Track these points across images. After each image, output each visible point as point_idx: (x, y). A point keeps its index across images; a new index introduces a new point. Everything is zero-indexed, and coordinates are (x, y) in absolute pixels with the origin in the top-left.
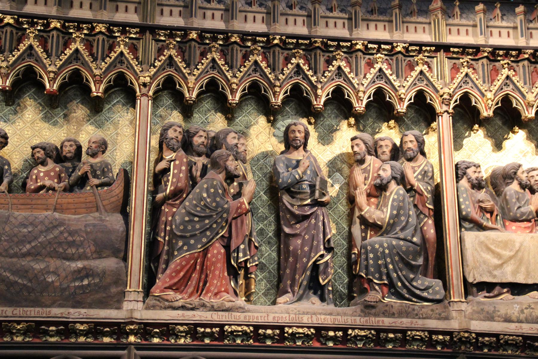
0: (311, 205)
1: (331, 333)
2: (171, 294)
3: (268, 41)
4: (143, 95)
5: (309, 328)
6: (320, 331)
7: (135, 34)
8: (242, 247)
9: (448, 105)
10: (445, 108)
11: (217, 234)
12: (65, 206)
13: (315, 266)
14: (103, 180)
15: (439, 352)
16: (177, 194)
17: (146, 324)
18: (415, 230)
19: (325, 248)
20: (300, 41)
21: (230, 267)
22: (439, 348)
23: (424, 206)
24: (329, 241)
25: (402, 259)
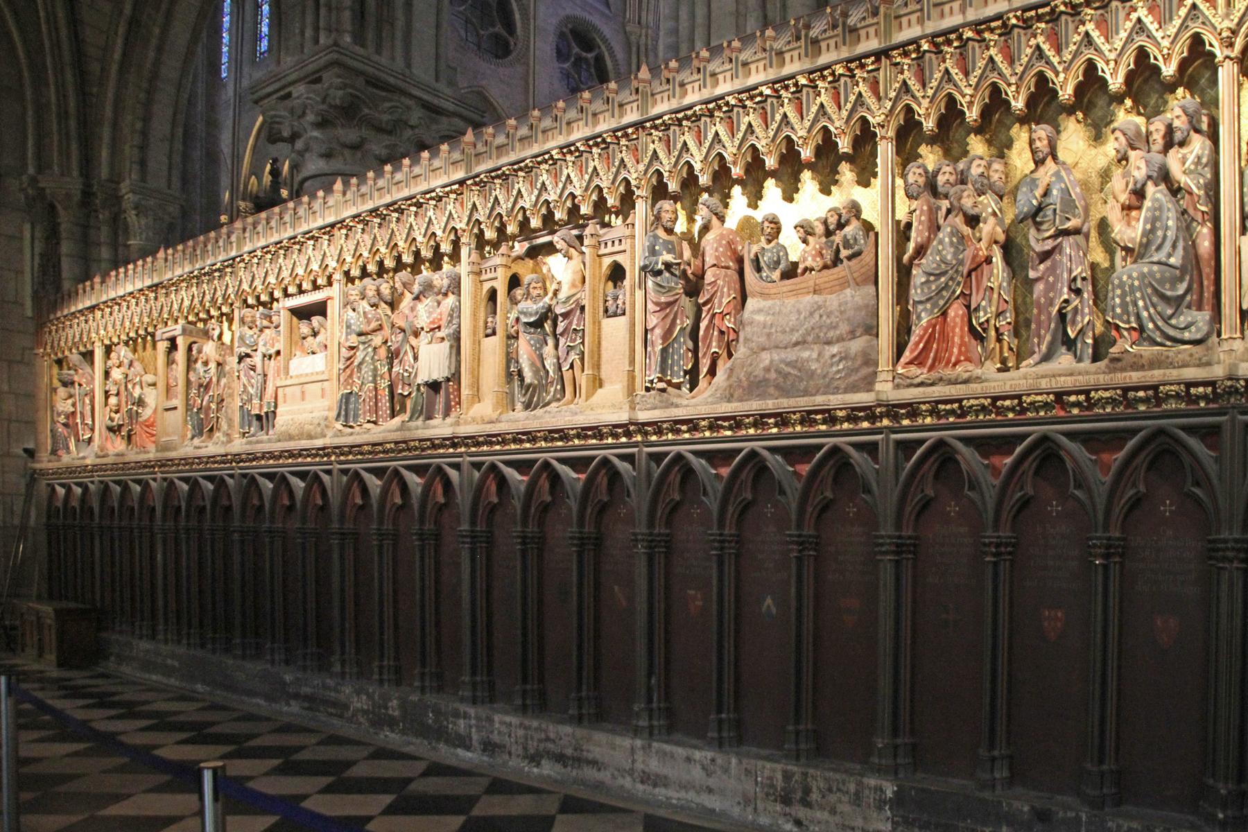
0: (1054, 237)
1: (1073, 398)
2: (914, 370)
3: (1005, 25)
4: (883, 138)
5: (1048, 394)
6: (1060, 396)
7: (873, 63)
8: (983, 303)
9: (1231, 45)
10: (1227, 52)
11: (954, 292)
12: (823, 286)
13: (1062, 316)
14: (856, 248)
15: (1202, 409)
16: (920, 251)
17: (894, 406)
18: (1174, 246)
19: (1070, 289)
20: (1040, 11)
21: (972, 329)
22: (1202, 405)
23: (1196, 209)
24: (1075, 279)
25: (1156, 291)
